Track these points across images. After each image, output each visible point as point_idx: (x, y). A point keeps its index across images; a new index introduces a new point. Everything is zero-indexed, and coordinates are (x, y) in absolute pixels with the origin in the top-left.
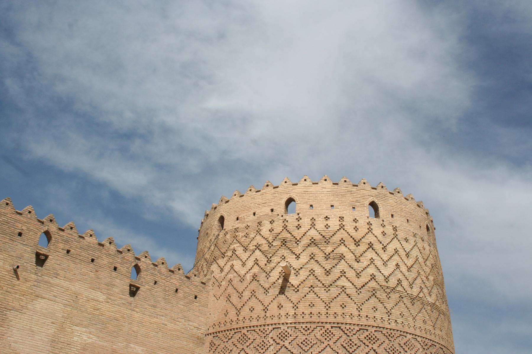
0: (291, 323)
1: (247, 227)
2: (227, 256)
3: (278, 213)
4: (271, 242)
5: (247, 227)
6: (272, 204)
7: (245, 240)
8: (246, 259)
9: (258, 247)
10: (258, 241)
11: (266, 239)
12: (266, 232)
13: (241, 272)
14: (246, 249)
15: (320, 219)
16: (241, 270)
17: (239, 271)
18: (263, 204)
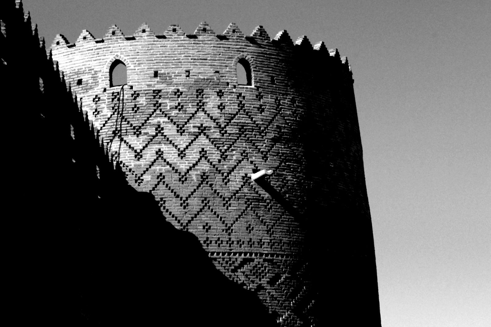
0: (267, 255)
1: (178, 93)
2: (146, 134)
3: (229, 81)
4: (223, 126)
5: (178, 93)
6: (215, 64)
7: (178, 114)
8: (184, 146)
9: (202, 130)
10: (203, 121)
11: (215, 120)
12: (214, 109)
13: (179, 166)
14: (181, 131)
15: (286, 102)
16: (180, 163)
17: (176, 163)
18: (201, 59)
